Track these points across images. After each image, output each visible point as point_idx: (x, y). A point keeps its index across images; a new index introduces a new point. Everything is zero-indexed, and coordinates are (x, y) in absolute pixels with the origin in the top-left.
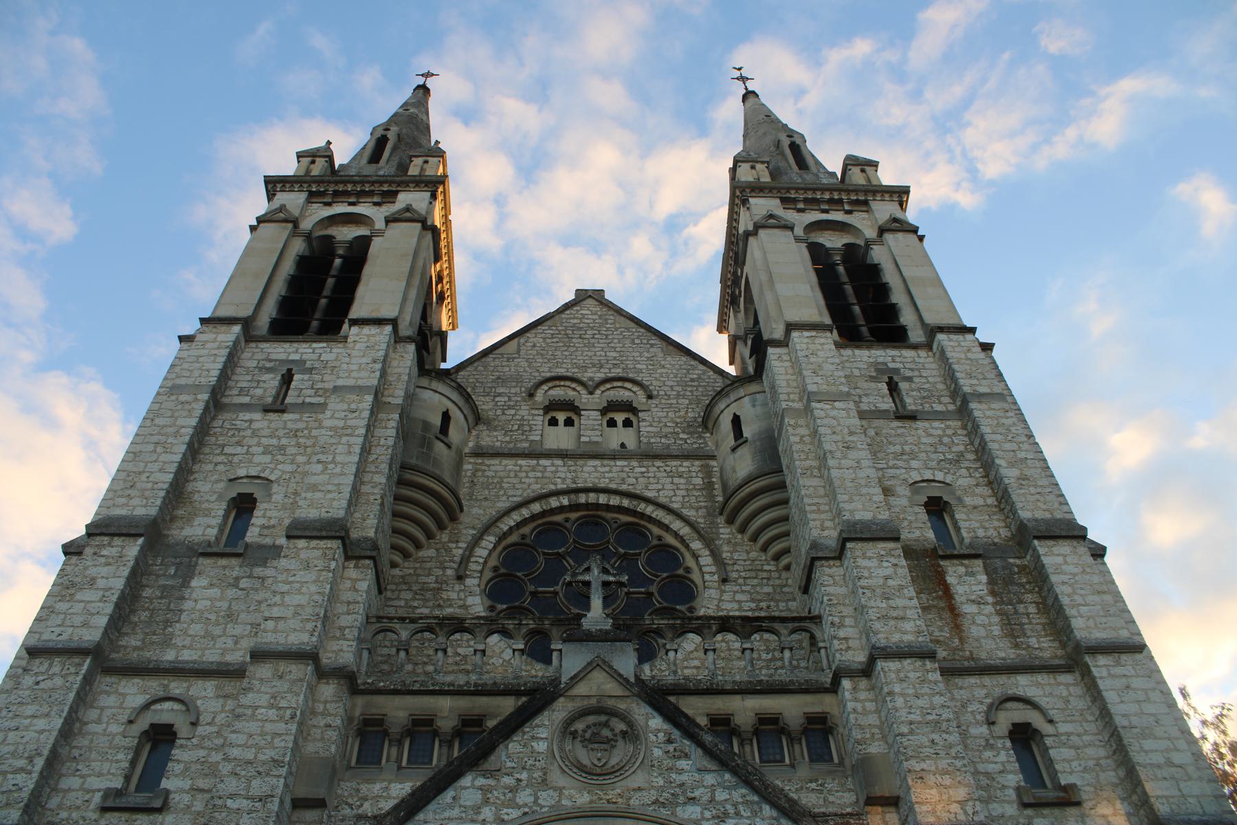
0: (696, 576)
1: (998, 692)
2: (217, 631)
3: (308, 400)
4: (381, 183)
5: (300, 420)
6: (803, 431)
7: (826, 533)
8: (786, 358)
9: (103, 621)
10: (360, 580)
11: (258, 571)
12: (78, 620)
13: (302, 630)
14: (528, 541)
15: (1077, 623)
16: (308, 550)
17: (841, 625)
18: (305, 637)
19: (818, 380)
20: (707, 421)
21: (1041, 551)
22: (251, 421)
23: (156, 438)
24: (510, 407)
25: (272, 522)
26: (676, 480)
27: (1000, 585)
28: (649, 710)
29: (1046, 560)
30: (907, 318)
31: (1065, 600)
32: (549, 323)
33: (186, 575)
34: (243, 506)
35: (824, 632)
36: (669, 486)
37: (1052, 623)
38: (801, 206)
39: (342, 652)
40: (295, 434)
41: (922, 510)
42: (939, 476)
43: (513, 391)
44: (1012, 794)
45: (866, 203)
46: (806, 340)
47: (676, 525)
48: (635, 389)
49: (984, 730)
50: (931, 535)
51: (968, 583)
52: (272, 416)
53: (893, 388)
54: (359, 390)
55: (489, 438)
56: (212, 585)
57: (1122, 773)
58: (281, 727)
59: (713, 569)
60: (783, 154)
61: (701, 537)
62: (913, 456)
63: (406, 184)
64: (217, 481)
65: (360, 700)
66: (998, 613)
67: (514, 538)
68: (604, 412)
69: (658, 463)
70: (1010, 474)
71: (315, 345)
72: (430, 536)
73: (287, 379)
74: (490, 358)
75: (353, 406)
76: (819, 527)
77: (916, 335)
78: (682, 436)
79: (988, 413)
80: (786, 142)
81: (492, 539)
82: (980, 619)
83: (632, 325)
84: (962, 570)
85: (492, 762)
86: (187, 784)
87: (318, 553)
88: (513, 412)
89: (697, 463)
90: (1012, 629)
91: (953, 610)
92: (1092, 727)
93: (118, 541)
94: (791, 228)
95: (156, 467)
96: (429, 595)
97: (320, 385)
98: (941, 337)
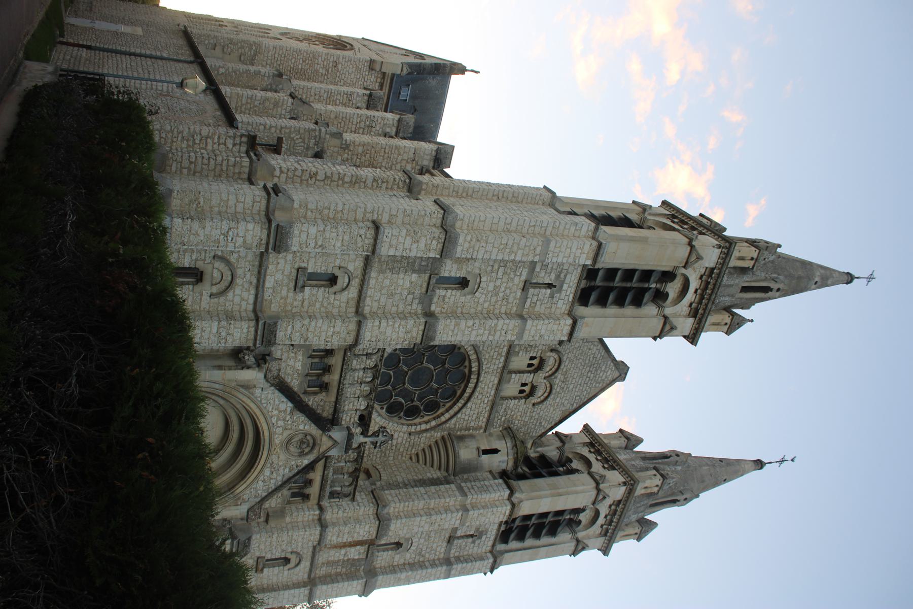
0: (417, 420)
1: (305, 556)
2: (383, 292)
3: (529, 300)
4: (705, 310)
5: (515, 298)
7: (392, 509)
11: (417, 301)
12: (394, 242)
13: (371, 337)
14: (456, 351)
15: (324, 587)
18: (368, 338)
19: (476, 515)
20: (509, 432)
22: (521, 275)
23: (510, 243)
25: (447, 300)
27: (353, 562)
28: (312, 459)
29: (355, 582)
30: (513, 544)
31: (335, 585)
32: (606, 355)
33: (419, 271)
34: (463, 283)
35: (345, 502)
37: (330, 575)
38: (613, 507)
40: (506, 298)
41: (397, 540)
45: (605, 535)
47: (447, 416)
48: (542, 398)
49: (290, 550)
51: (355, 553)
52: (521, 286)
53: (472, 536)
56: (411, 283)
57: (265, 586)
58: (323, 338)
64: (480, 269)
66: (339, 561)
69: (488, 408)
70: (403, 575)
71: (572, 295)
73: (550, 286)
75: (509, 332)
77: (501, 547)
80: (678, 498)
82: (337, 554)
83: (591, 395)
87: (414, 335)
89: (484, 425)
90: (329, 563)
92: (285, 580)
93: (440, 246)
94: (594, 503)
97: (538, 303)
98: (491, 560)
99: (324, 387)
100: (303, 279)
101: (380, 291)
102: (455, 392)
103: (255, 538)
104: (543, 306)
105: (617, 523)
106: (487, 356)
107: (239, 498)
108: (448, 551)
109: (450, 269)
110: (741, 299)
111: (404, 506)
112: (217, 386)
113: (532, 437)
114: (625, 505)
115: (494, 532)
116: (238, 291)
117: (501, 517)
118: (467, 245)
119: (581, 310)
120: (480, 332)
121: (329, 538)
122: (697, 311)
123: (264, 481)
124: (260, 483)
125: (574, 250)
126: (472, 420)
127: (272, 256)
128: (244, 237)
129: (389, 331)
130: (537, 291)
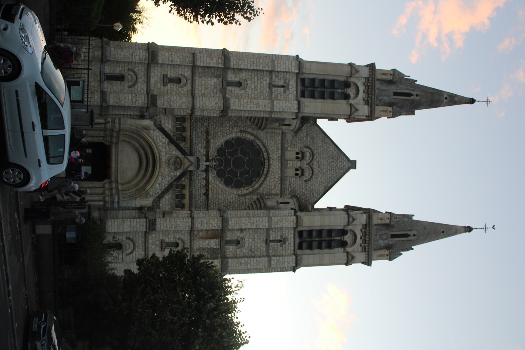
0: (242, 189)
1: (186, 242)
2: (203, 87)
3: (274, 94)
4: (371, 100)
5: (266, 92)
6: (262, 215)
7: (229, 215)
8: (290, 215)
9: (202, 65)
10: (216, 114)
11: (219, 92)
12: (202, 60)
16: (221, 104)
17: (203, 214)
18: (198, 106)
19: (276, 220)
20: (294, 196)
21: (218, 260)
22: (266, 80)
23: (255, 61)
24: (301, 141)
26: (273, 186)
30: (308, 251)
32: (339, 152)
33: (217, 77)
34: (239, 84)
36: (271, 184)
39: (196, 114)
40: (261, 92)
41: (236, 238)
42: (246, 245)
43: (308, 142)
44: (164, 239)
45: (365, 251)
46: (292, 220)
48: (309, 177)
49: (178, 237)
50: (228, 239)
52: (268, 86)
53: (280, 241)
54: (273, 106)
55: (289, 137)
56: (214, 83)
58: (178, 105)
59: (243, 193)
60: (404, 230)
61: (253, 191)
62: (253, 240)
63: (371, 108)
64: (245, 77)
65: (189, 117)
66: (205, 248)
67: (255, 144)
68: (300, 167)
69: (279, 182)
71: (295, 92)
72: (254, 122)
73: (283, 87)
74: (322, 134)
76: (230, 214)
77: (299, 252)
78: (290, 189)
79: (264, 261)
80: (409, 233)
81: (253, 138)
82: (204, 244)
84: (217, 243)
85: (170, 144)
86: (169, 88)
88: (300, 142)
89: (279, 192)
91: (206, 238)
93: (223, 62)
95: (246, 63)
96: (236, 124)
97: (279, 95)
99: (184, 139)
100: (167, 80)
101: (201, 86)
102: (259, 173)
103: (158, 220)
104: (282, 97)
105: (369, 241)
106: (271, 149)
107: (148, 194)
108: (268, 250)
109: (231, 77)
110: (396, 99)
111: (236, 214)
112: (133, 128)
113: (310, 203)
114: (369, 227)
115: (292, 240)
116: (139, 85)
117: (292, 224)
118: (235, 62)
119: (302, 100)
120: (252, 105)
121: (197, 226)
122: (368, 101)
123: (159, 184)
124: (158, 185)
125: (287, 65)
126: (272, 189)
127: (152, 65)
128: (139, 56)
129: (207, 103)
130: (276, 89)
